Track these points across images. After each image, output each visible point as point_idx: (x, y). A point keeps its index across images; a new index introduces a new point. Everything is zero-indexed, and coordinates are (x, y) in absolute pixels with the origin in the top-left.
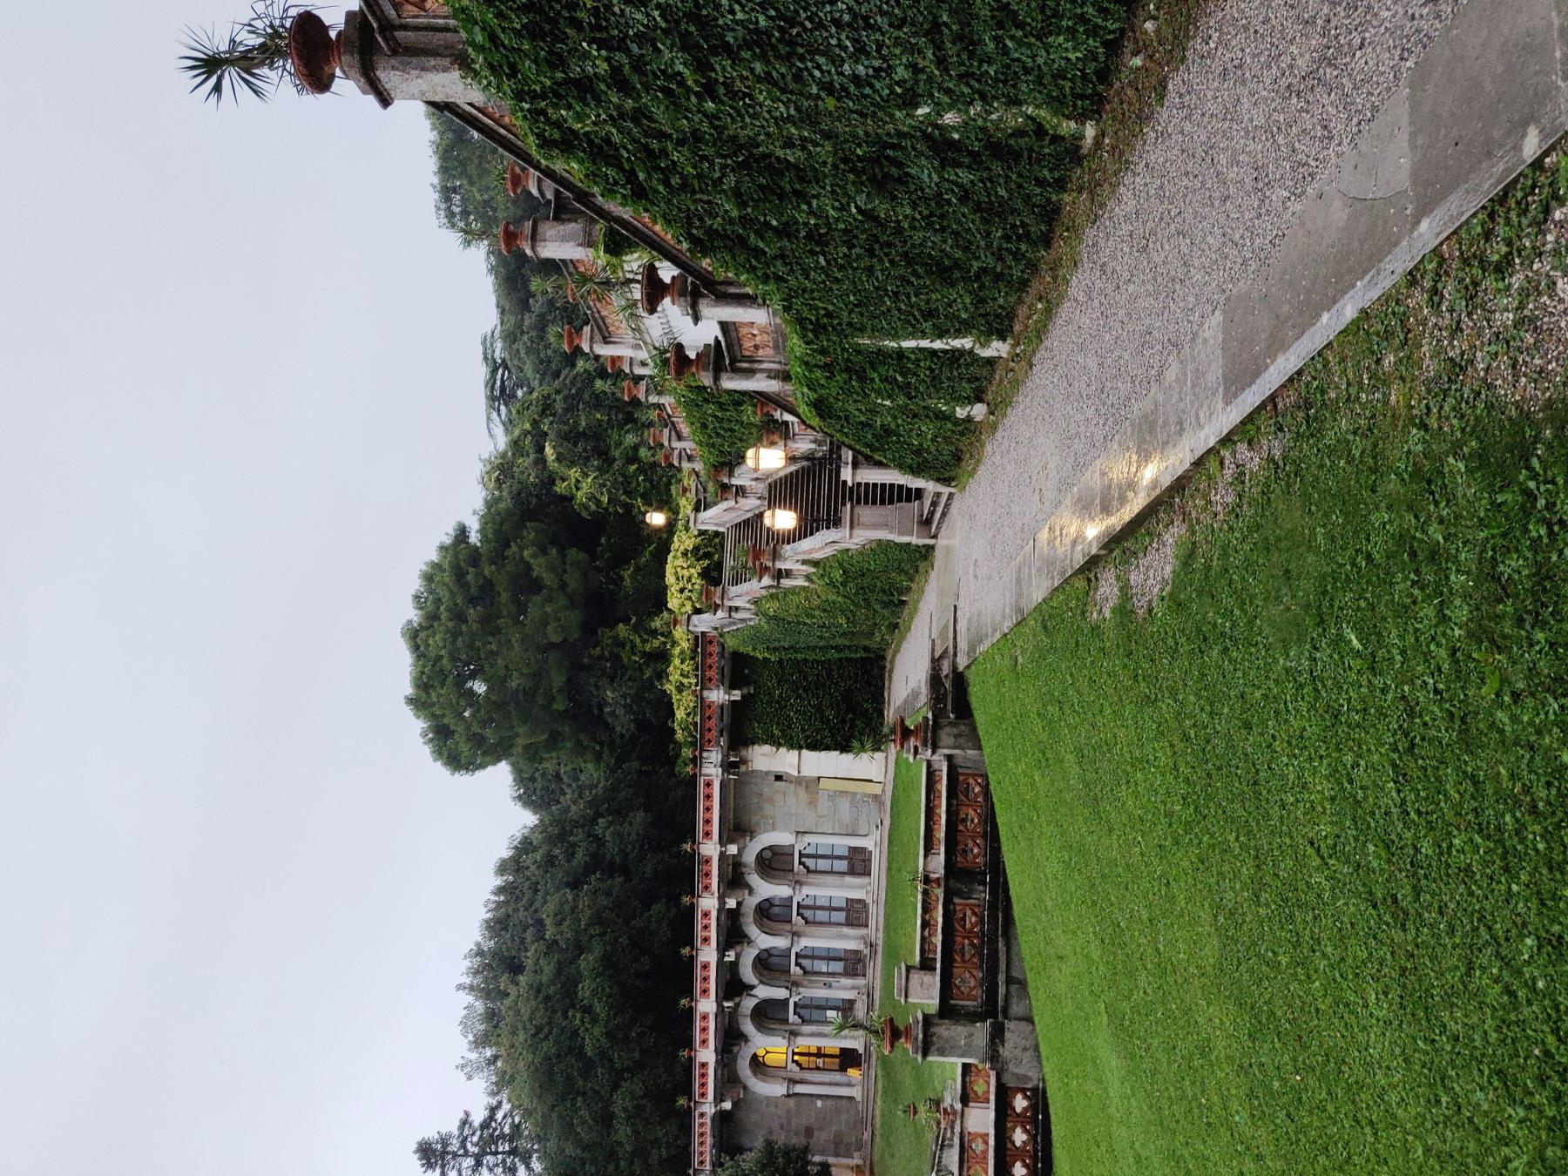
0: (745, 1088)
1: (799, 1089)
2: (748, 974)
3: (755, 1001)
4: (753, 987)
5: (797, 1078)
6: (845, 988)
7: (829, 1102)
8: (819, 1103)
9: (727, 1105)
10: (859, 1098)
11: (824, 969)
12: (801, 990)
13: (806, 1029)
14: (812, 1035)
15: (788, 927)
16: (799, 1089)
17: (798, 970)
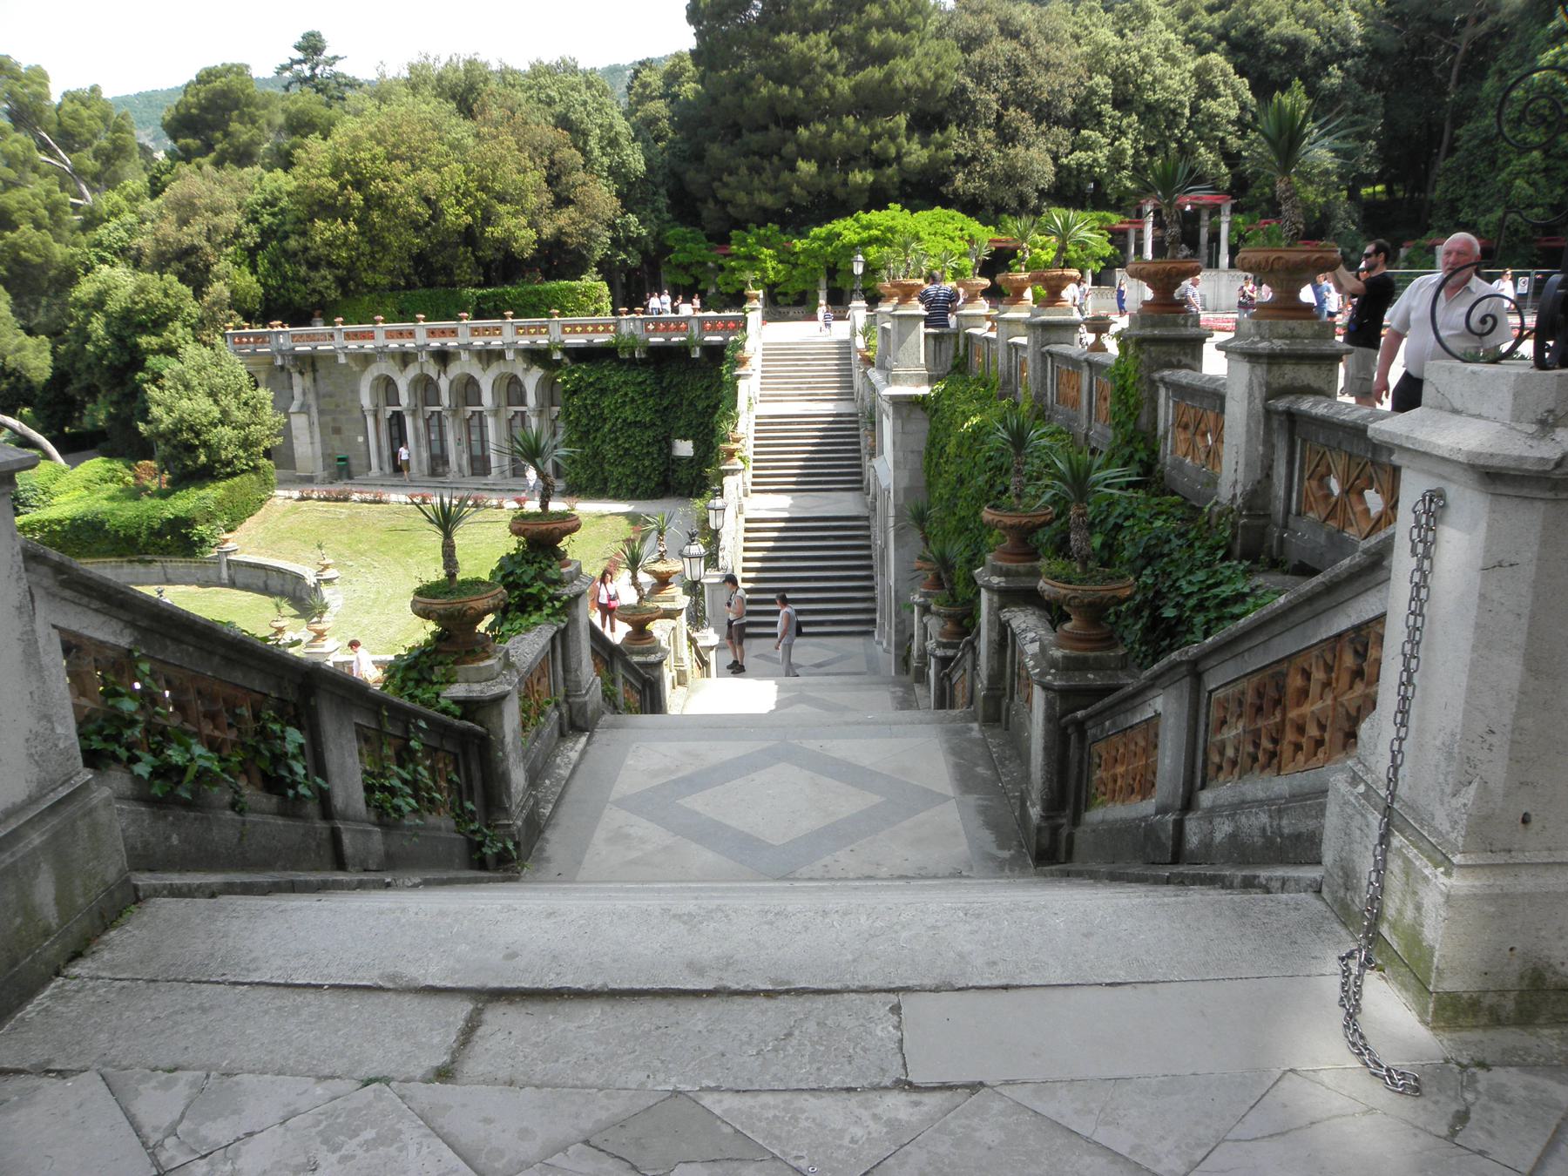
0: (363, 371)
1: (370, 421)
2: (455, 370)
3: (435, 377)
4: (445, 373)
5: (380, 416)
6: (459, 457)
7: (363, 448)
8: (361, 439)
9: (342, 360)
10: (370, 474)
11: (473, 437)
12: (450, 419)
13: (421, 424)
14: (416, 429)
15: (503, 403)
16: (370, 421)
17: (469, 414)
